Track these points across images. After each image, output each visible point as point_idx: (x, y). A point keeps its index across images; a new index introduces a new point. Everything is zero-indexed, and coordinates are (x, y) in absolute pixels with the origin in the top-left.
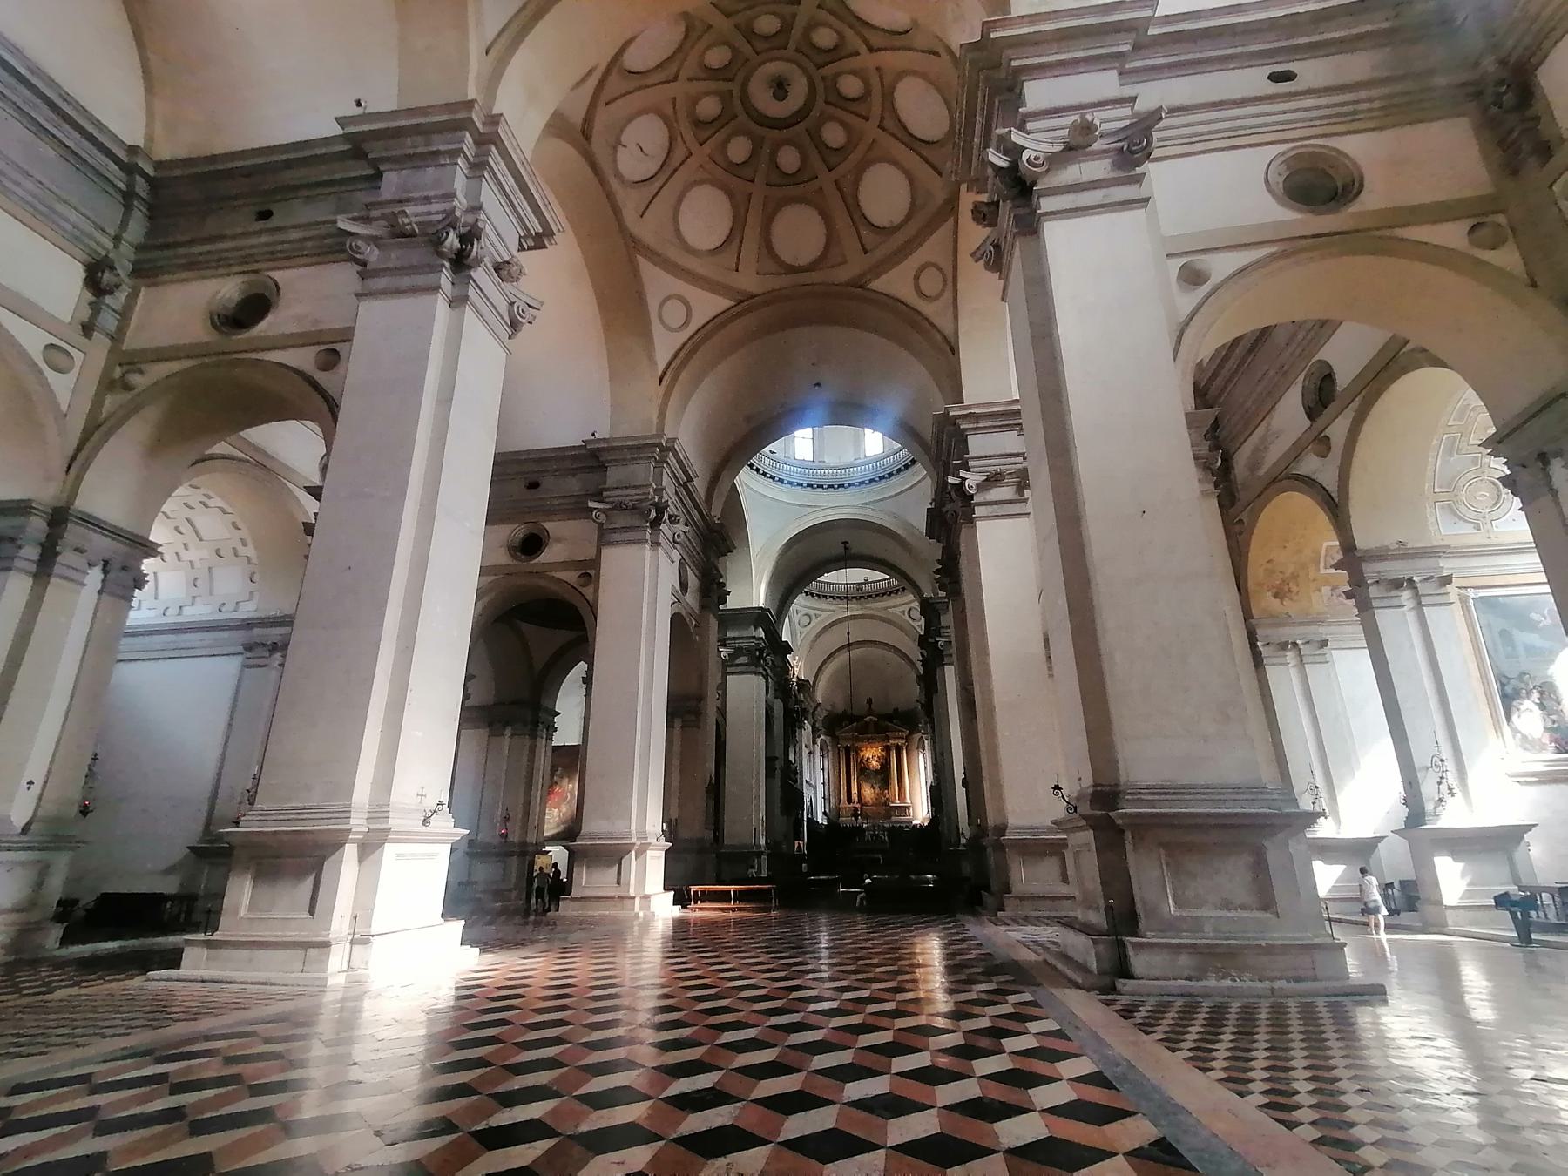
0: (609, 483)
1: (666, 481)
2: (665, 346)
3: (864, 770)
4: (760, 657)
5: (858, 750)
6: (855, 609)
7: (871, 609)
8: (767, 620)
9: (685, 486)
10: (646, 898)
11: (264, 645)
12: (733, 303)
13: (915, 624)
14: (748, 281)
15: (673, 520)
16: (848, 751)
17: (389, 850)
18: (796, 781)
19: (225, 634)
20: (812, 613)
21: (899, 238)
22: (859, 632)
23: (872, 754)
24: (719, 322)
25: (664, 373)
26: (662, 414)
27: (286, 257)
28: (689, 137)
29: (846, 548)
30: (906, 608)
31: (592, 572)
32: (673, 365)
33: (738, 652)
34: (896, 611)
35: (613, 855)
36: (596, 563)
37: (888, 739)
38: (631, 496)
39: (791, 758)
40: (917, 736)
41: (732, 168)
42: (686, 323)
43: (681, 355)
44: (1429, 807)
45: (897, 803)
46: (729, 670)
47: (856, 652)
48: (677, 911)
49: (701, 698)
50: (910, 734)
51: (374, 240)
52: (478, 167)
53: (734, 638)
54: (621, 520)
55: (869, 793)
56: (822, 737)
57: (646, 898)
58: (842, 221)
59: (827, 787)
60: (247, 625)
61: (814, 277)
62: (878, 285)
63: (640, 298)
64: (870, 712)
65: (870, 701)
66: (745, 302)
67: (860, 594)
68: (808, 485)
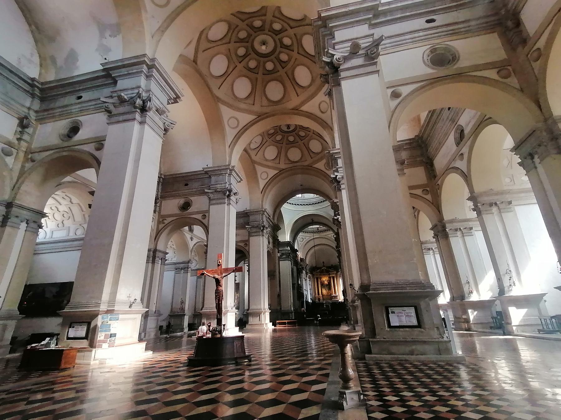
0: (250, 220)
1: (265, 219)
2: (262, 184)
3: (323, 285)
4: (289, 255)
5: (320, 278)
6: (316, 236)
7: (321, 235)
8: (290, 244)
9: (269, 218)
10: (266, 324)
11: (179, 268)
12: (278, 172)
14: (283, 166)
15: (267, 228)
17: (228, 314)
18: (301, 290)
19: (170, 266)
21: (320, 155)
22: (317, 242)
23: (325, 279)
24: (275, 177)
25: (262, 190)
26: (262, 201)
27: (193, 195)
28: (267, 138)
29: (312, 221)
31: (247, 243)
32: (264, 188)
33: (283, 254)
34: (330, 236)
35: (258, 314)
36: (248, 241)
37: (330, 274)
38: (256, 224)
39: (300, 283)
41: (278, 142)
42: (267, 177)
43: (266, 186)
44: (506, 289)
45: (334, 295)
46: (280, 260)
47: (316, 248)
48: (273, 327)
49: (275, 271)
51: (212, 193)
52: (230, 175)
53: (281, 250)
54: (254, 230)
55: (325, 292)
56: (309, 274)
57: (266, 324)
58: (306, 152)
60: (175, 264)
61: (298, 164)
62: (316, 166)
63: (256, 173)
65: (323, 262)
66: (281, 171)
67: (318, 231)
68: (300, 205)
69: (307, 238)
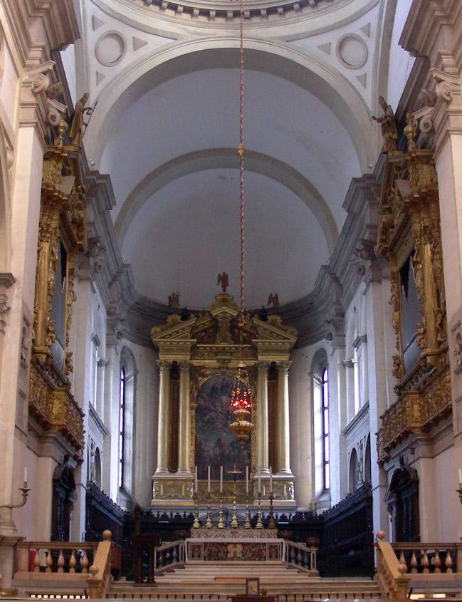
13: (351, 75)
16: (174, 370)
20: (129, 34)
30: (333, 38)
37: (254, 351)
40: (311, 350)
50: (296, 347)
59: (129, 443)
64: (225, 301)
65: (224, 280)
69: (154, 43)
